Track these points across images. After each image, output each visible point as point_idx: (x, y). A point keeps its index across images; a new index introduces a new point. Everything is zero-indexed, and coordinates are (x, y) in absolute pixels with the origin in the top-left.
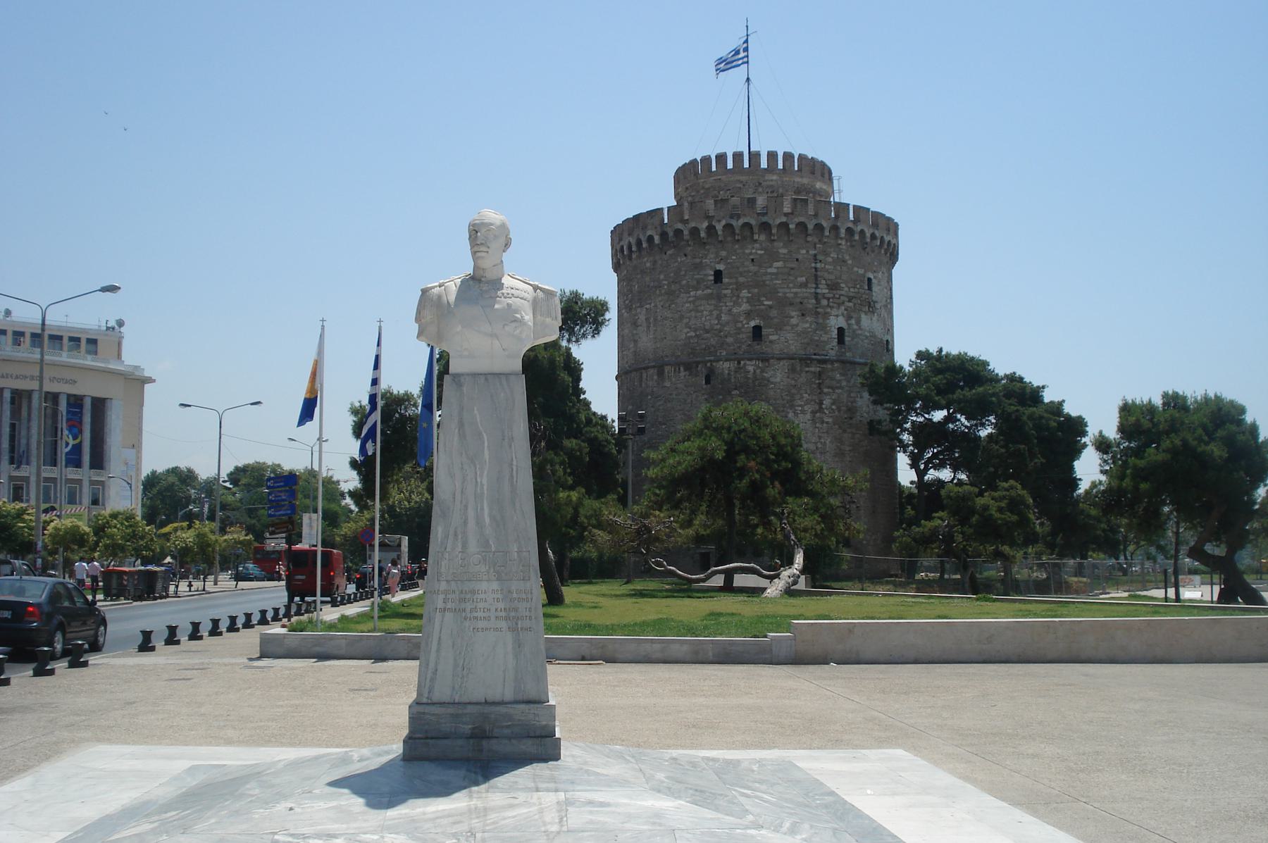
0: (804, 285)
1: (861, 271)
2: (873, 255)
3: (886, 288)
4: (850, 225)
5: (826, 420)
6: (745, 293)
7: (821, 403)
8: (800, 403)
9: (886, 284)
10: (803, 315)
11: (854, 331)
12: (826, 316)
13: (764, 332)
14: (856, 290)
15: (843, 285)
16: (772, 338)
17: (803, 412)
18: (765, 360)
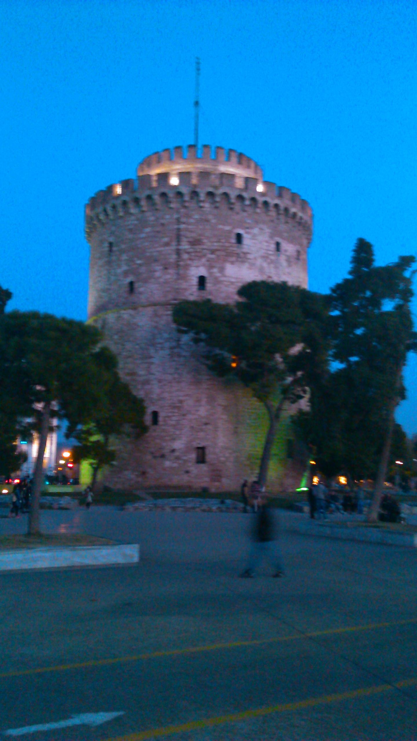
0: (167, 244)
1: (227, 228)
2: (245, 214)
3: (267, 242)
4: (211, 189)
5: (184, 353)
6: (124, 257)
7: (179, 340)
8: (161, 341)
9: (267, 239)
10: (166, 268)
11: (216, 278)
12: (187, 267)
13: (136, 285)
14: (221, 244)
15: (205, 241)
16: (142, 289)
17: (162, 348)
18: (135, 309)
